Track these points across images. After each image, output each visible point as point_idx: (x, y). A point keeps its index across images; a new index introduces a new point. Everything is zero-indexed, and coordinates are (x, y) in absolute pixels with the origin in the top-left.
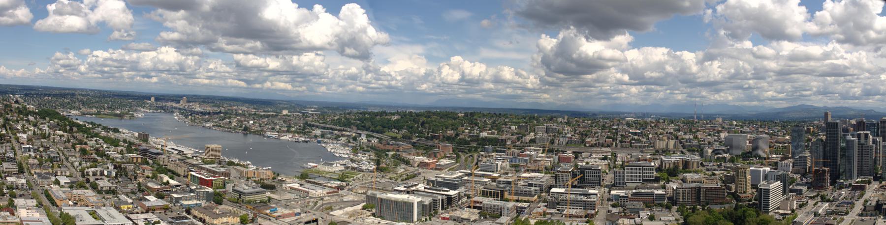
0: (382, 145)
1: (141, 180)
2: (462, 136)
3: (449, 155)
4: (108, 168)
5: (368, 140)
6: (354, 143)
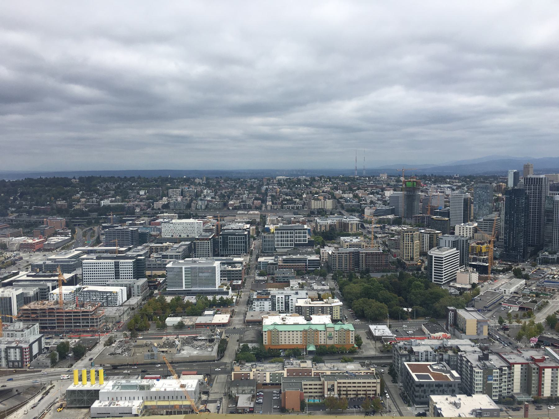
2: (77, 207)
3: (62, 231)
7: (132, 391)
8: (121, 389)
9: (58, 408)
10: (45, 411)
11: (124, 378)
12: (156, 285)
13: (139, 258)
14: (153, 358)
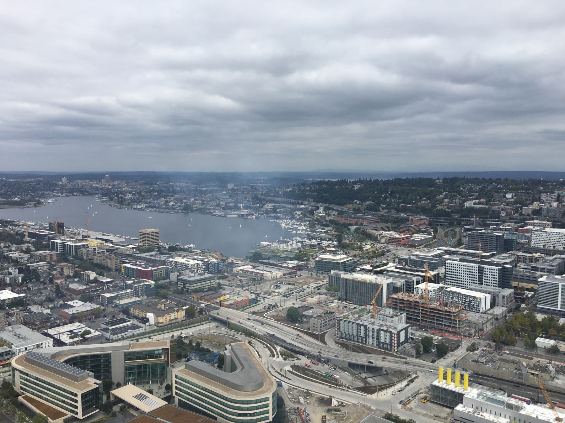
0: (344, 218)
1: (59, 282)
2: (440, 207)
4: (10, 274)
5: (327, 214)
6: (310, 218)
7: (499, 406)
8: (486, 401)
9: (422, 399)
10: (411, 398)
11: (488, 390)
12: (523, 298)
13: (505, 266)
14: (522, 379)
